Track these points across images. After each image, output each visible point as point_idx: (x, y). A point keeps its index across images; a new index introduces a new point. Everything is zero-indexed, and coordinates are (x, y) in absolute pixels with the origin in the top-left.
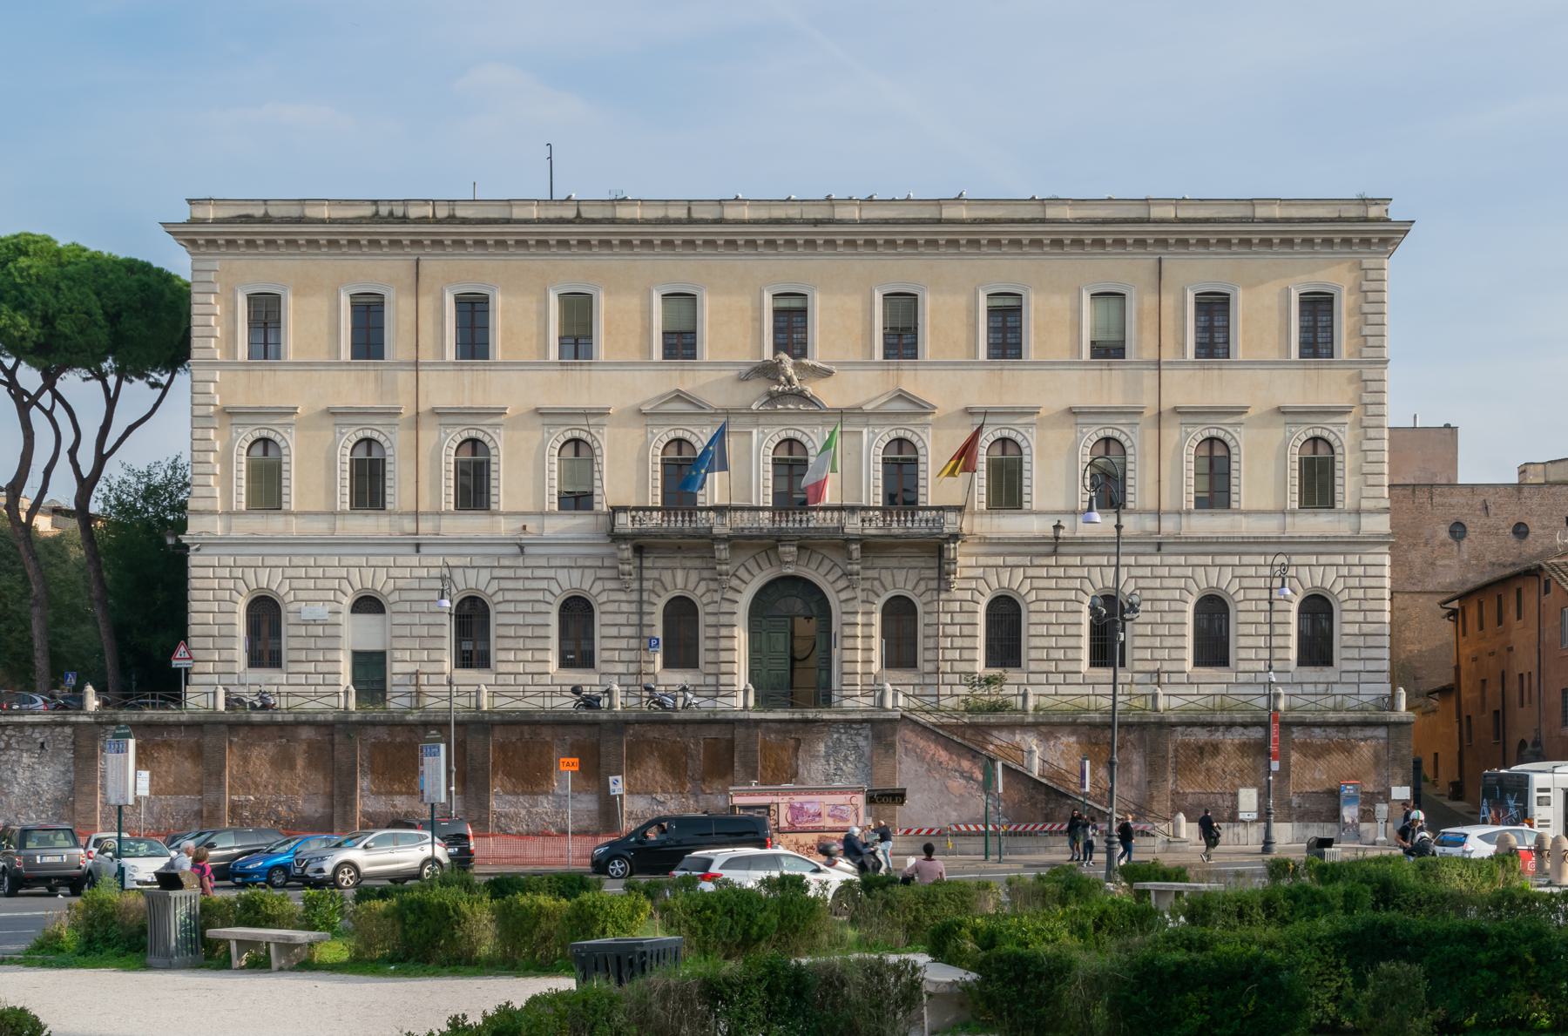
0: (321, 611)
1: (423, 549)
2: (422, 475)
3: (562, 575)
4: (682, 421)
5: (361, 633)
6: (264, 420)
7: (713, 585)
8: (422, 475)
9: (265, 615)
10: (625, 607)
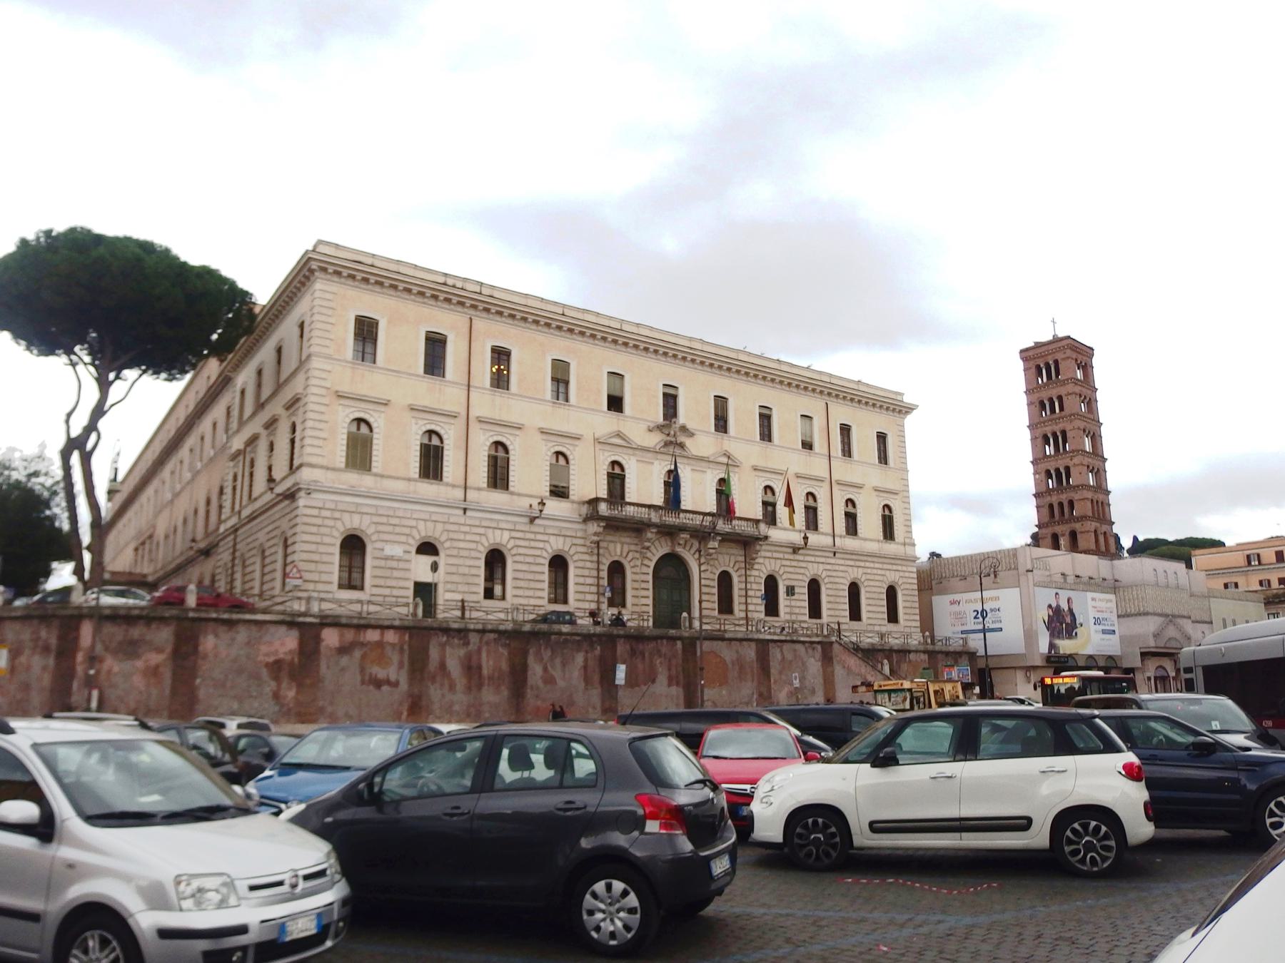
0: (397, 551)
1: (468, 513)
2: (465, 461)
3: (552, 539)
4: (620, 450)
5: (421, 569)
6: (363, 405)
7: (637, 555)
8: (465, 461)
9: (353, 546)
10: (589, 565)
